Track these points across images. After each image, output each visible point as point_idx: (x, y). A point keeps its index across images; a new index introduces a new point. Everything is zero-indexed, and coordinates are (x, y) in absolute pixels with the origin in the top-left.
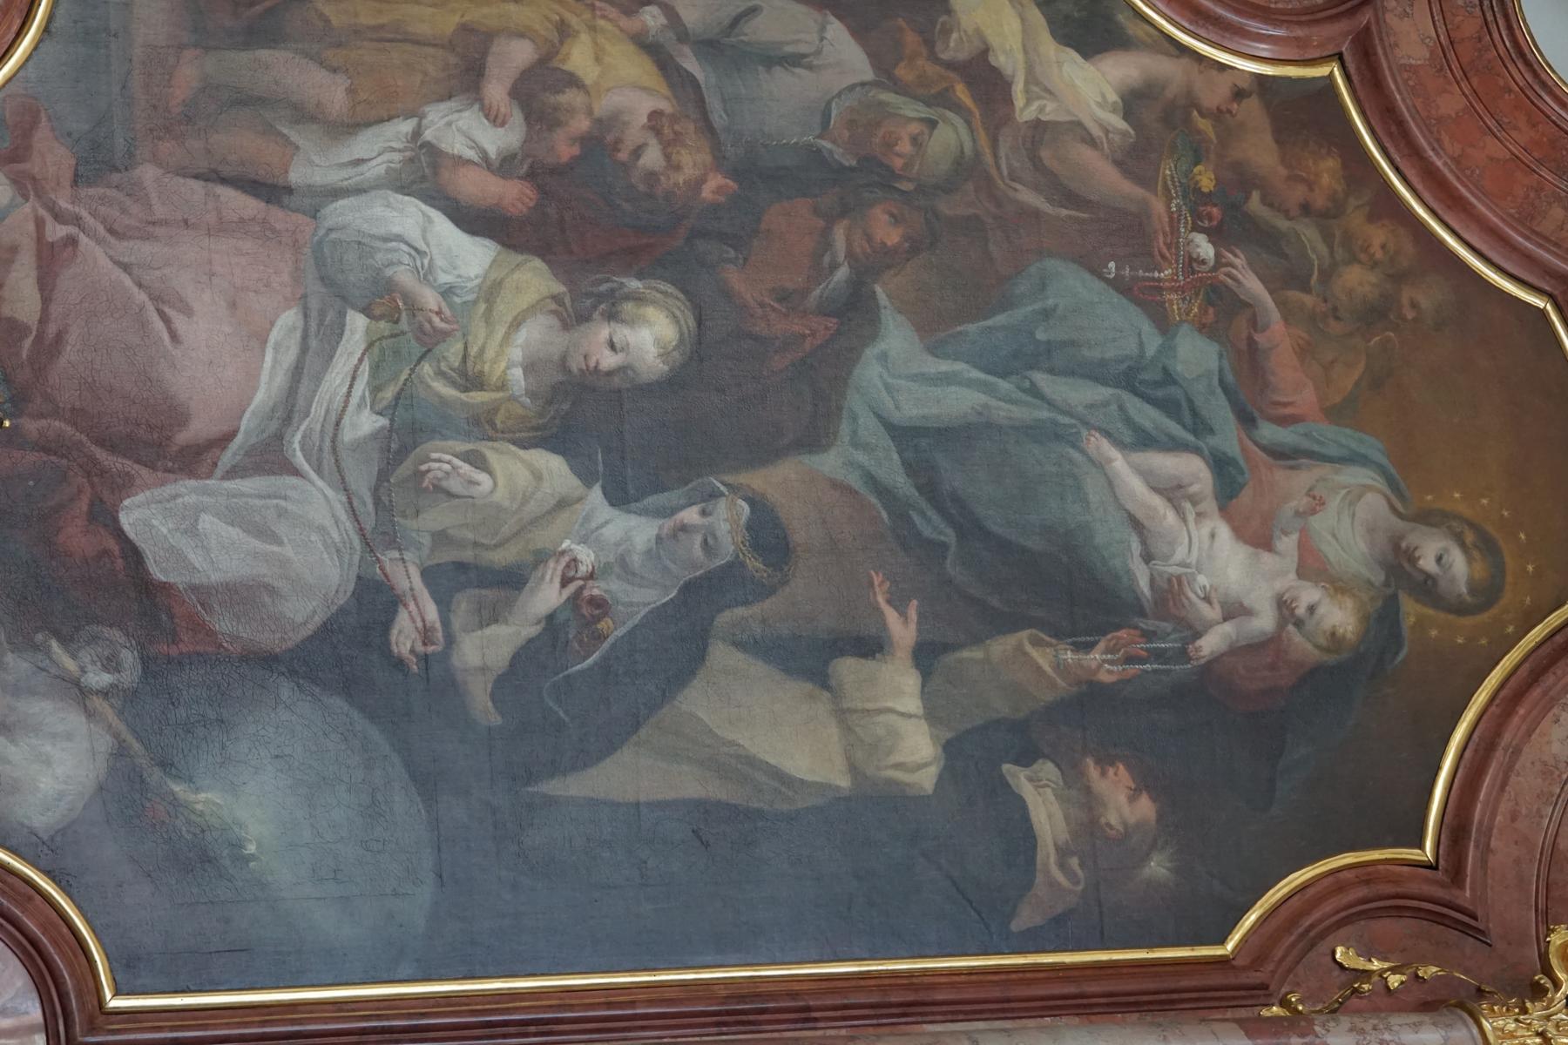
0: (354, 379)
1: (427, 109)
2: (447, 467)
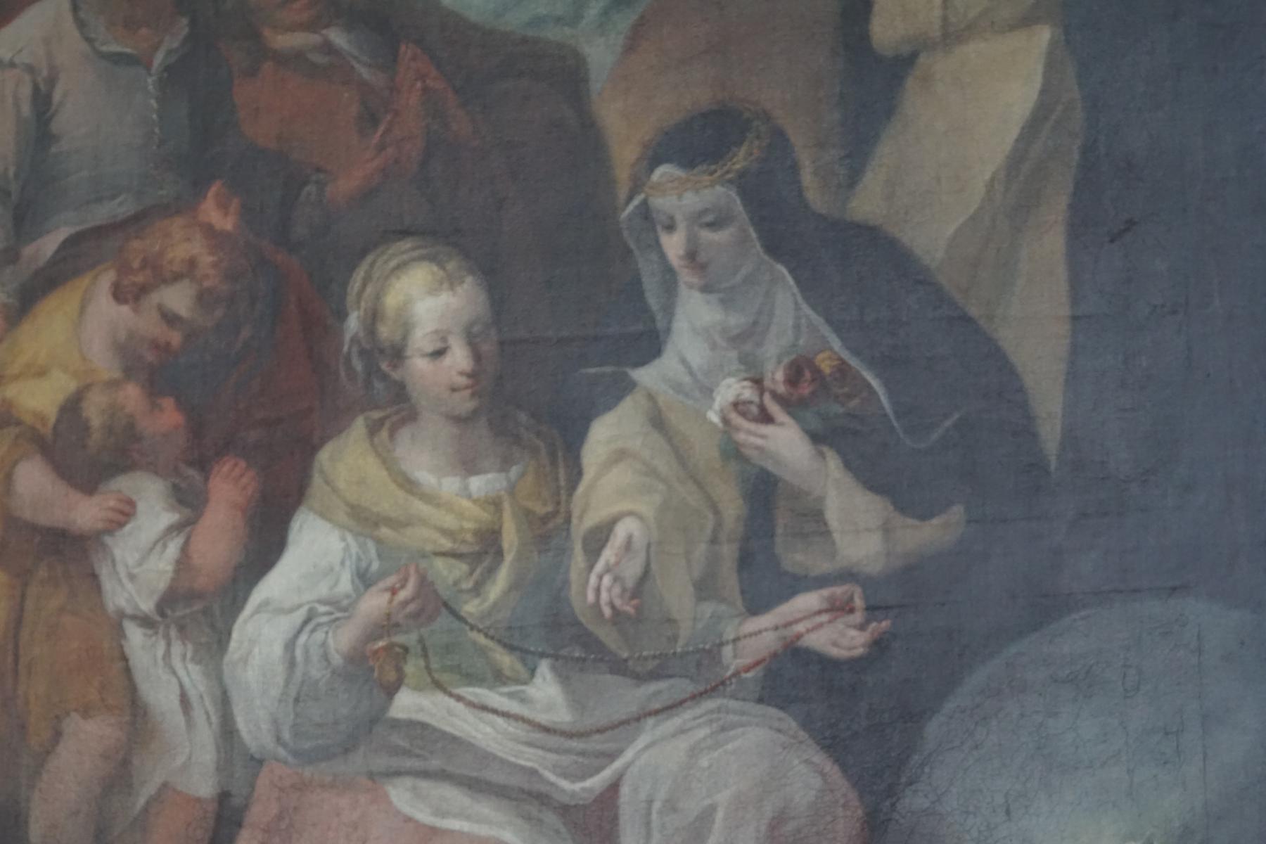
0: (484, 708)
1: (111, 607)
2: (607, 580)
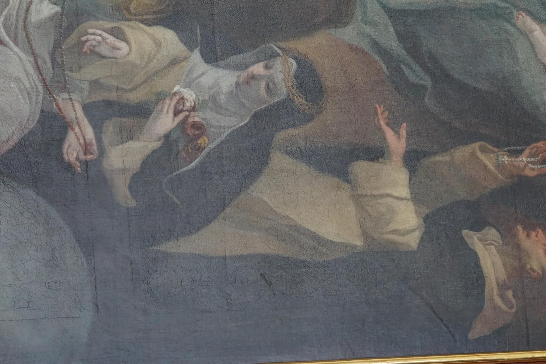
2: (99, 38)
